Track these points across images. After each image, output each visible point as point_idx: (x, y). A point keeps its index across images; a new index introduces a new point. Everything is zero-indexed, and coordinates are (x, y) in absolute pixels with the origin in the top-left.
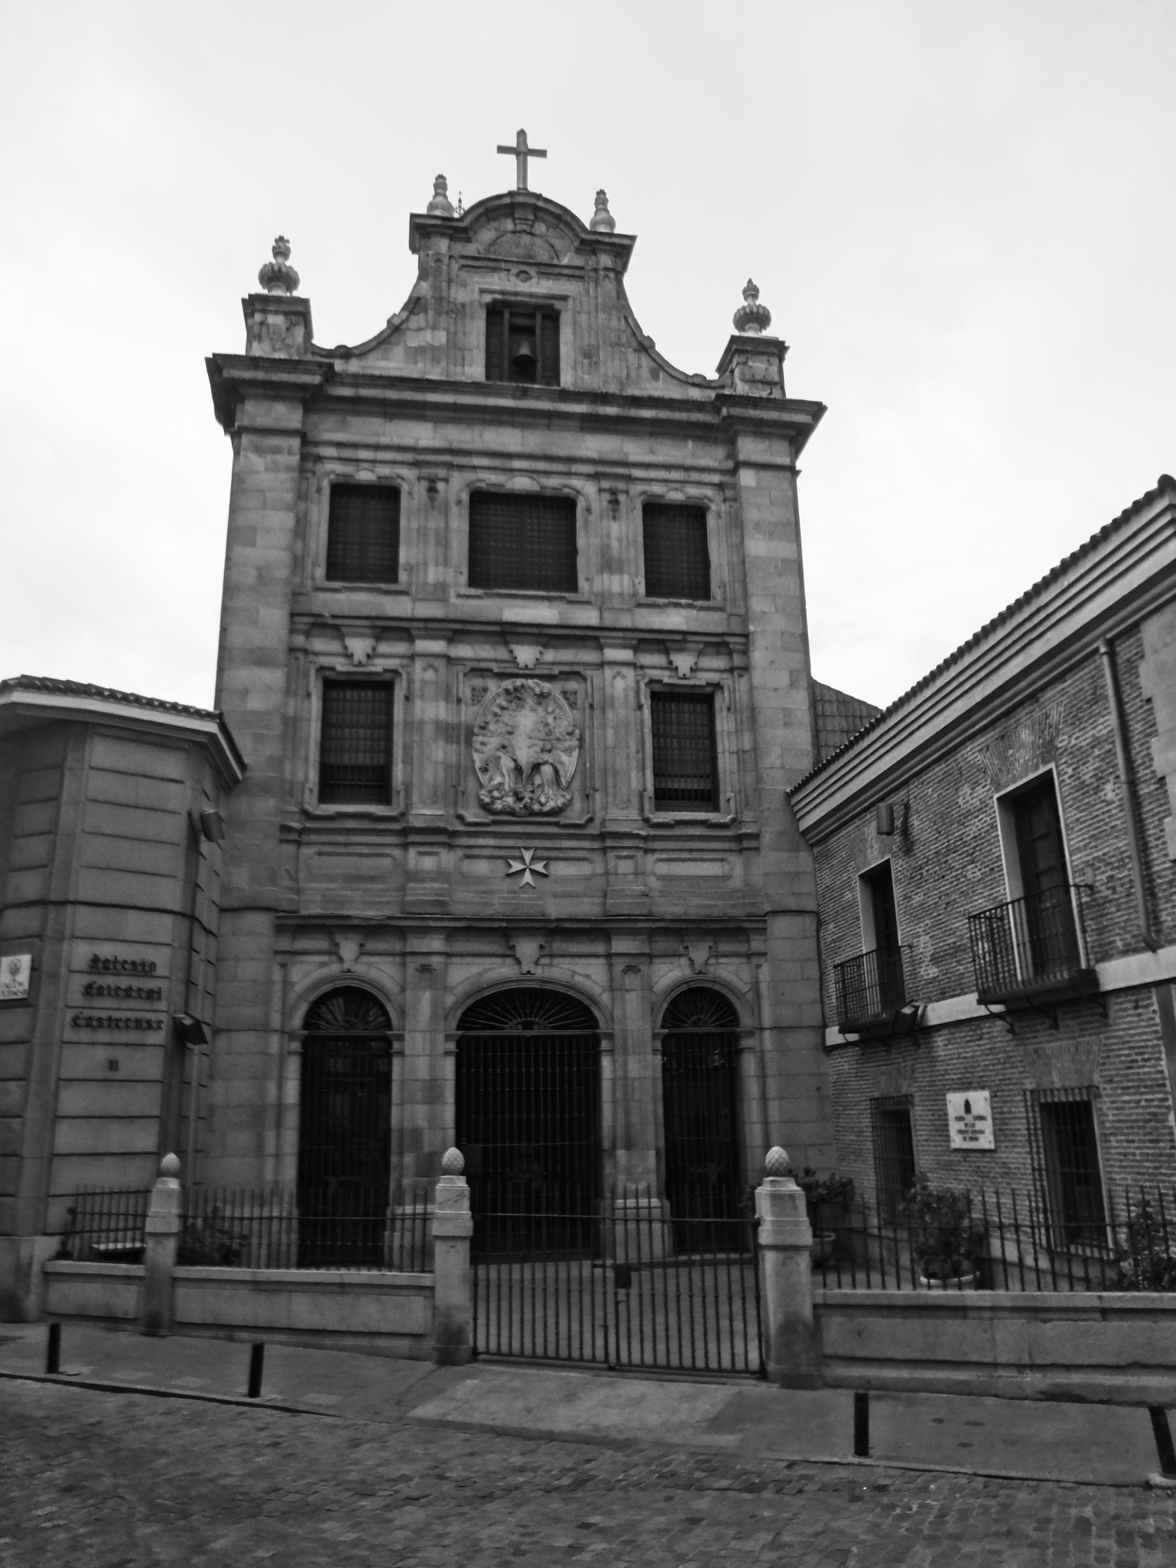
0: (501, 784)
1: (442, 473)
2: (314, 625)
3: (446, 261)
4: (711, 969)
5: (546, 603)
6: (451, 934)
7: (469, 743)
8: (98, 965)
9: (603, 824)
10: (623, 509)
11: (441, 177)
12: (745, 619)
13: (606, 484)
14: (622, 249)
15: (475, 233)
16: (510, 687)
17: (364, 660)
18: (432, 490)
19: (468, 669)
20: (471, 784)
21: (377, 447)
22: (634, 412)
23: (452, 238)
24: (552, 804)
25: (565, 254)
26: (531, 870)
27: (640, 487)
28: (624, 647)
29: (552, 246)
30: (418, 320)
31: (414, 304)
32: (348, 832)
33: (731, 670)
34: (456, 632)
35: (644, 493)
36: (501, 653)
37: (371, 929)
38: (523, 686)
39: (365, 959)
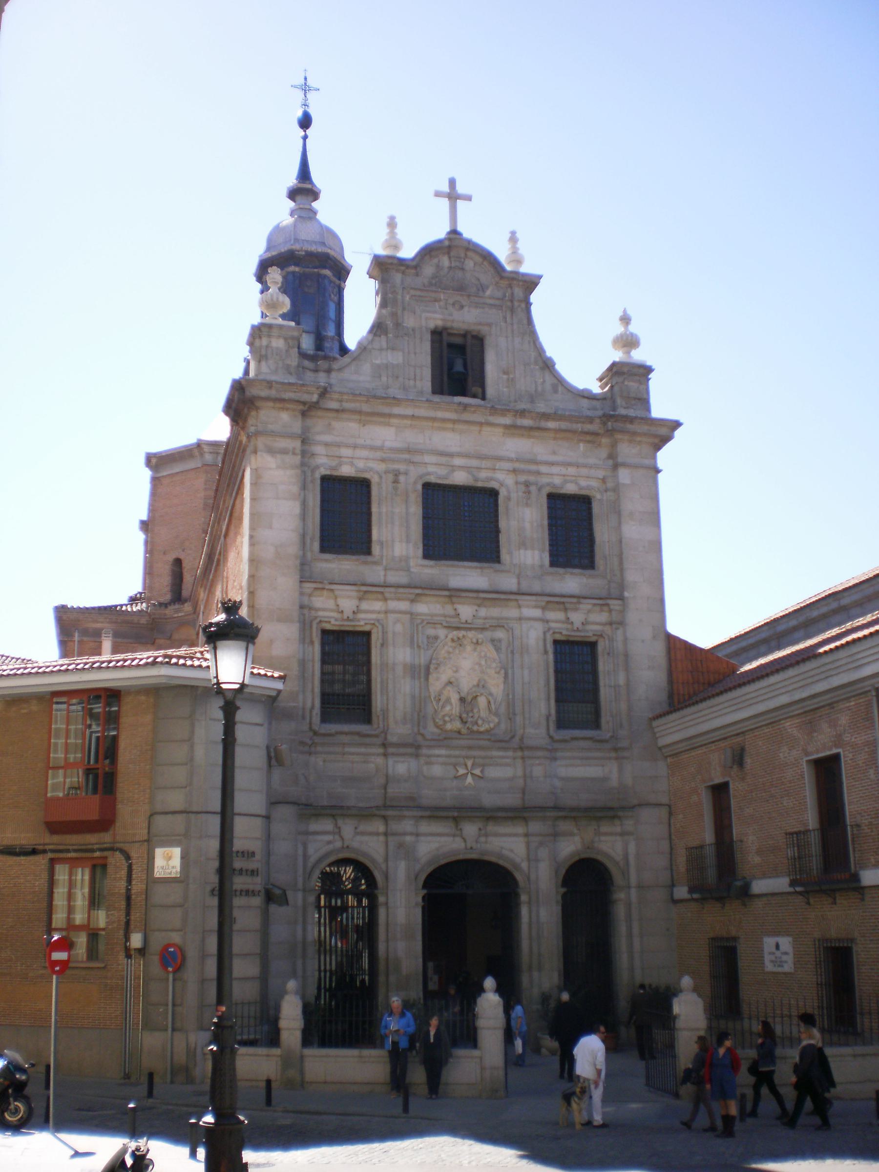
3: (400, 292)
4: (596, 845)
7: (427, 679)
9: (522, 739)
12: (622, 586)
14: (531, 283)
16: (455, 638)
17: (351, 616)
18: (396, 481)
19: (425, 622)
20: (430, 710)
22: (543, 424)
23: (403, 273)
25: (487, 287)
26: (472, 774)
28: (536, 607)
29: (479, 280)
33: (611, 624)
35: (548, 484)
36: (449, 610)
38: (464, 636)
39: (358, 838)
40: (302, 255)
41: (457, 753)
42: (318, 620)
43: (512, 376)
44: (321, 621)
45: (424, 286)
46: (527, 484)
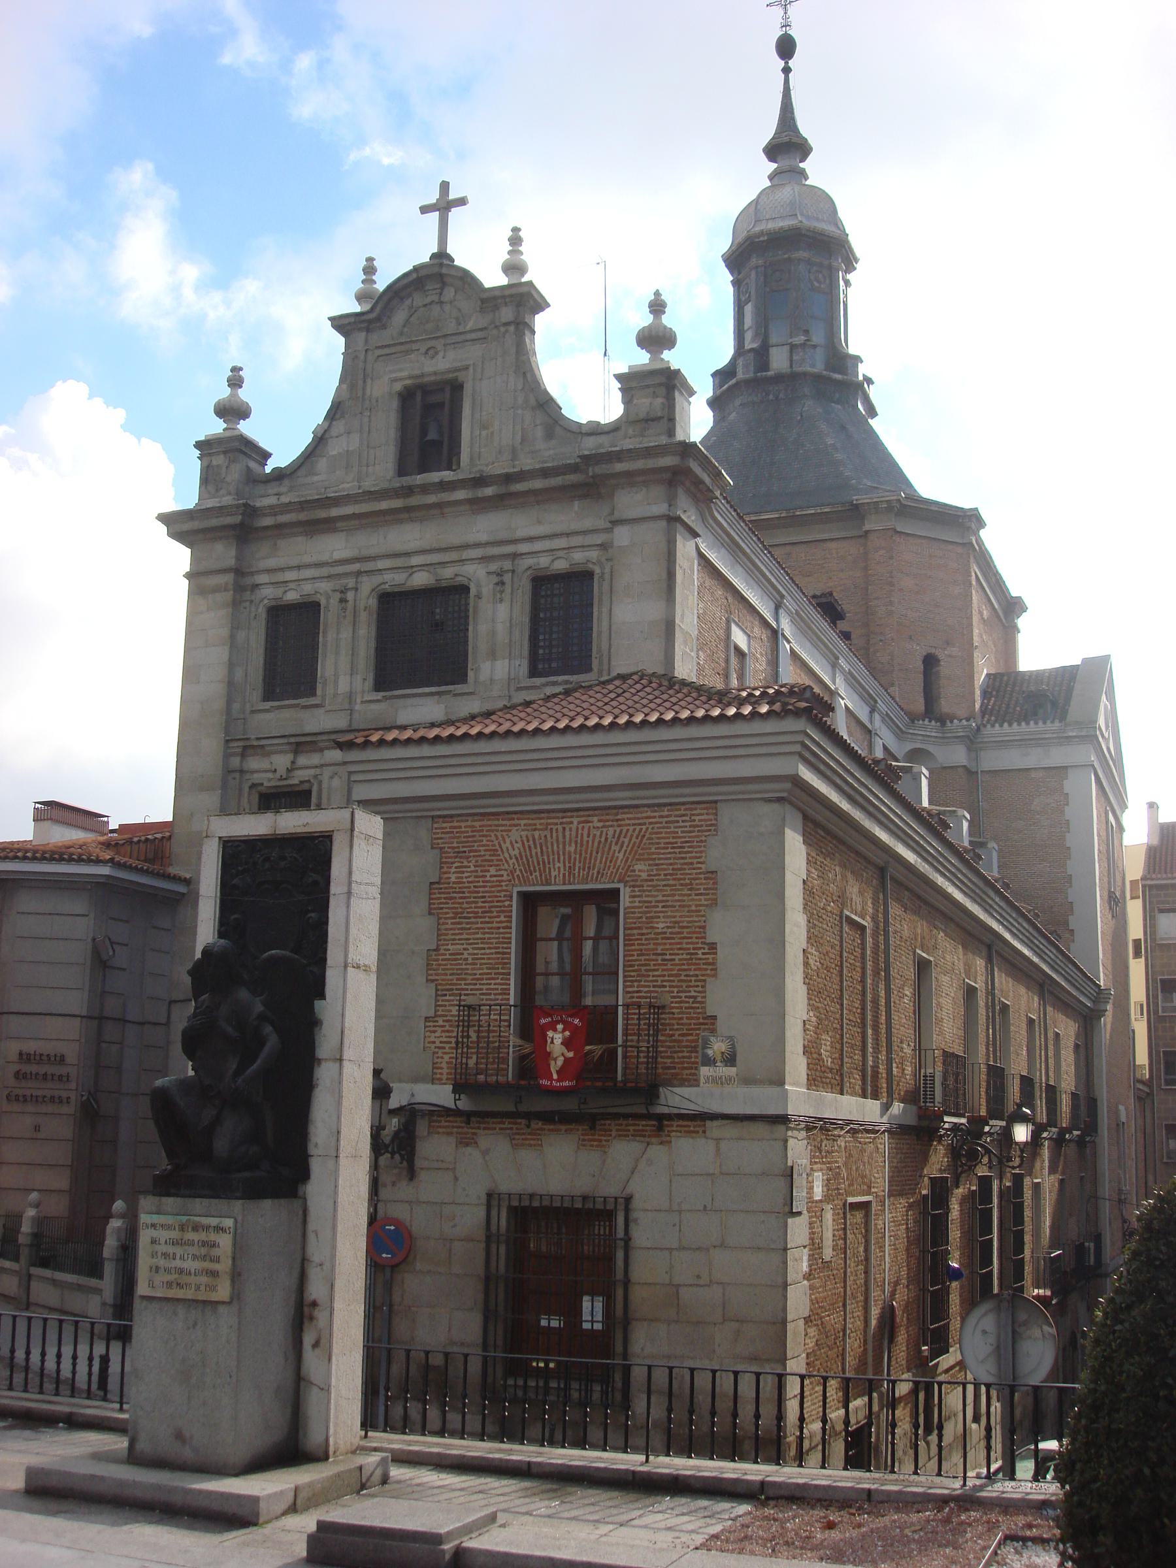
1: (351, 582)
2: (245, 748)
5: (436, 697)
8: (24, 1057)
11: (370, 260)
13: (494, 567)
15: (389, 317)
18: (343, 601)
21: (299, 567)
23: (368, 330)
27: (530, 561)
30: (339, 427)
31: (335, 412)
40: (763, 241)
42: (250, 783)
44: (253, 786)
45: (393, 339)
46: (499, 574)
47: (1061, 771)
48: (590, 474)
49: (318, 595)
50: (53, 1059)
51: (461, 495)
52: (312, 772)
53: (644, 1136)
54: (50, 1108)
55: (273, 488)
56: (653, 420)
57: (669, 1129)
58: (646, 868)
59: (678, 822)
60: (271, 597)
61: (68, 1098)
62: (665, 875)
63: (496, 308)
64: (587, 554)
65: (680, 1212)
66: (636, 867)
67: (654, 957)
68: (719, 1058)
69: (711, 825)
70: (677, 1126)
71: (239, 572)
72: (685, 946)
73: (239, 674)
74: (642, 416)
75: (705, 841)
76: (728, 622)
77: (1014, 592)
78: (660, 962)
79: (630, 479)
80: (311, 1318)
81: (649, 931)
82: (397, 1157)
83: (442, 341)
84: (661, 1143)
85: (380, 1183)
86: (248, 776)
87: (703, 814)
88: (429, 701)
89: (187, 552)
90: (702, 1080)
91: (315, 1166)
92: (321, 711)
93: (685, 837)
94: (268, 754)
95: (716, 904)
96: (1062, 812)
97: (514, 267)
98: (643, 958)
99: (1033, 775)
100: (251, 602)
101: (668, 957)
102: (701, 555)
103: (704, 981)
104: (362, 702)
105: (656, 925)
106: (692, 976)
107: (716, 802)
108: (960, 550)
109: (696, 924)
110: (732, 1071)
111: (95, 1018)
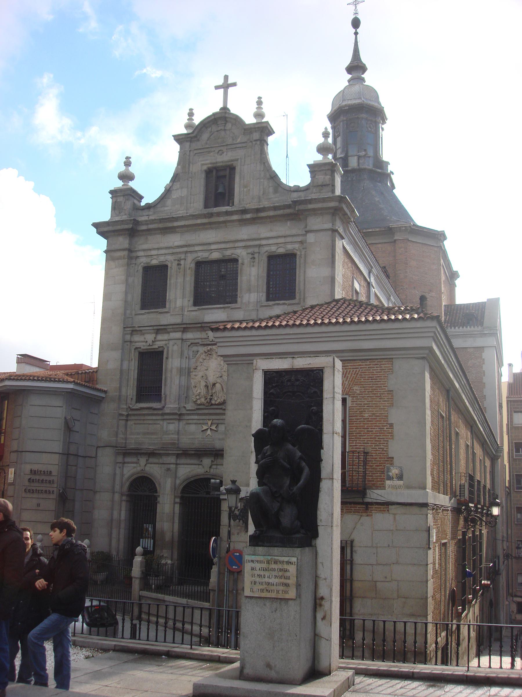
0: (200, 393)
1: (183, 256)
5: (223, 310)
6: (178, 456)
10: (257, 260)
13: (250, 250)
15: (201, 136)
18: (179, 264)
19: (190, 344)
23: (191, 142)
24: (219, 401)
30: (177, 185)
31: (175, 178)
32: (144, 415)
34: (184, 328)
37: (151, 454)
38: (211, 349)
39: (148, 465)
41: (204, 417)
42: (134, 347)
43: (249, 188)
44: (136, 348)
47: (481, 349)
48: (297, 209)
49: (167, 262)
50: (46, 473)
51: (235, 217)
52: (164, 342)
53: (359, 512)
54: (45, 496)
55: (146, 212)
56: (325, 185)
57: (372, 509)
58: (359, 388)
59: (374, 367)
60: (145, 262)
61: (53, 491)
62: (368, 392)
63: (251, 133)
64: (293, 246)
65: (377, 547)
66: (354, 388)
67: (363, 430)
68: (395, 476)
69: (390, 369)
70: (375, 508)
71: (130, 251)
72: (378, 425)
73: (129, 298)
74: (320, 183)
75: (387, 377)
76: (353, 278)
77: (455, 269)
78: (366, 432)
79: (315, 212)
80: (321, 605)
81: (361, 418)
82: (241, 521)
83: (226, 147)
84: (367, 516)
85: (231, 533)
86: (134, 344)
87: (386, 364)
88: (220, 311)
89: (105, 241)
90: (387, 487)
91: (321, 530)
92: (169, 314)
93: (378, 375)
94: (143, 334)
95: (393, 406)
96: (482, 367)
97: (259, 115)
98: (358, 430)
99: (469, 350)
100: (135, 264)
101: (370, 430)
102: (344, 247)
103: (388, 441)
104: (188, 311)
105: (364, 415)
106: (382, 439)
107: (392, 359)
108: (436, 249)
109: (383, 415)
110: (401, 483)
111: (66, 454)
